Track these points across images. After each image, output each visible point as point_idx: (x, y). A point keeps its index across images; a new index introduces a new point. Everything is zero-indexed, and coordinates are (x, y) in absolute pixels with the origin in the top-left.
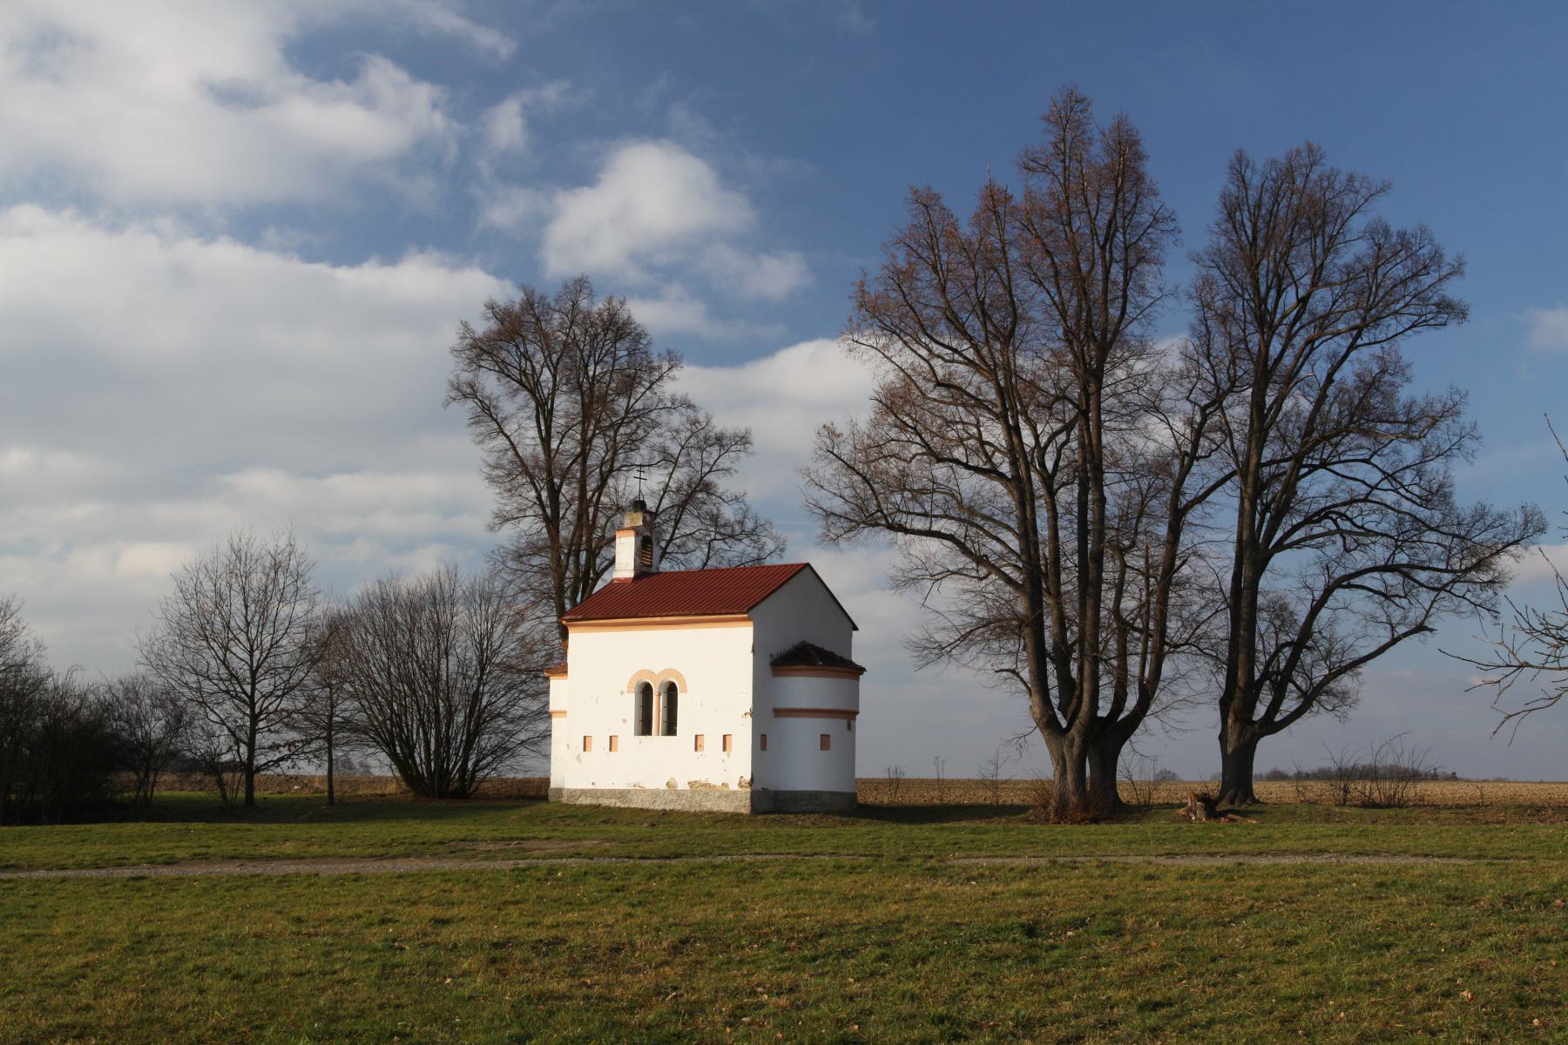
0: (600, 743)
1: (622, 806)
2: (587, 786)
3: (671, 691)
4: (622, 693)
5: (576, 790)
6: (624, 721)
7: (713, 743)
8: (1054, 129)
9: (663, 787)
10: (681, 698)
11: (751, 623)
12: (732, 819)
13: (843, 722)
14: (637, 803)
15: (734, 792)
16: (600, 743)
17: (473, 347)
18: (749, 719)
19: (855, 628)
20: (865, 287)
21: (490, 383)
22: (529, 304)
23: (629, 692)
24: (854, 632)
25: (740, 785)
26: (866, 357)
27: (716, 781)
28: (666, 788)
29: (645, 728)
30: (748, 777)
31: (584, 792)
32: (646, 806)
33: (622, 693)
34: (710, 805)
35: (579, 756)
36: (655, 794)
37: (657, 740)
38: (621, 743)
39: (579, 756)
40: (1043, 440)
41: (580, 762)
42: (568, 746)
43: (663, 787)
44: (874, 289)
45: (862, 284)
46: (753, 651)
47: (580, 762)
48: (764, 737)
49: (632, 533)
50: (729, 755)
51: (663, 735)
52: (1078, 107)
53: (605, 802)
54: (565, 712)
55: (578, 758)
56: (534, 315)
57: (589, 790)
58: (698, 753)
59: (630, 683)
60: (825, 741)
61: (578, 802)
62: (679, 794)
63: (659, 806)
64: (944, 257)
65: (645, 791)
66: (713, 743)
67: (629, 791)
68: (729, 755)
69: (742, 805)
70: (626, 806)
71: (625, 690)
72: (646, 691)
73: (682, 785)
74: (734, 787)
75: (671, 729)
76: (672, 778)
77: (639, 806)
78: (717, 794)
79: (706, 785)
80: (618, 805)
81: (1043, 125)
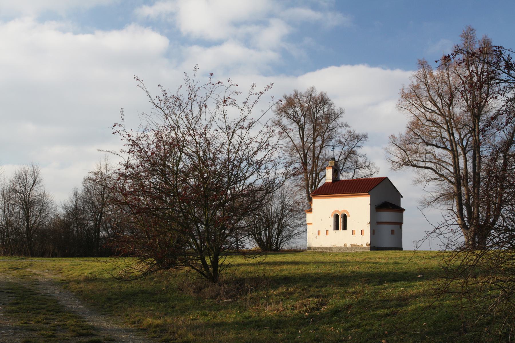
0: (323, 233)
3: (345, 217)
6: (330, 226)
8: (464, 39)
9: (343, 246)
10: (348, 219)
11: (369, 196)
13: (399, 226)
15: (365, 247)
16: (323, 233)
17: (279, 110)
18: (369, 225)
19: (402, 197)
20: (404, 91)
21: (285, 121)
22: (296, 95)
24: (402, 198)
25: (367, 245)
26: (404, 112)
29: (337, 228)
30: (369, 243)
37: (341, 232)
38: (329, 233)
40: (462, 137)
43: (343, 246)
44: (406, 91)
45: (403, 90)
46: (370, 204)
48: (374, 230)
49: (331, 168)
52: (471, 32)
54: (312, 224)
55: (316, 237)
56: (298, 99)
60: (393, 232)
62: (348, 248)
64: (429, 81)
65: (337, 247)
72: (337, 217)
73: (349, 245)
74: (365, 246)
75: (345, 228)
79: (356, 245)
81: (460, 38)
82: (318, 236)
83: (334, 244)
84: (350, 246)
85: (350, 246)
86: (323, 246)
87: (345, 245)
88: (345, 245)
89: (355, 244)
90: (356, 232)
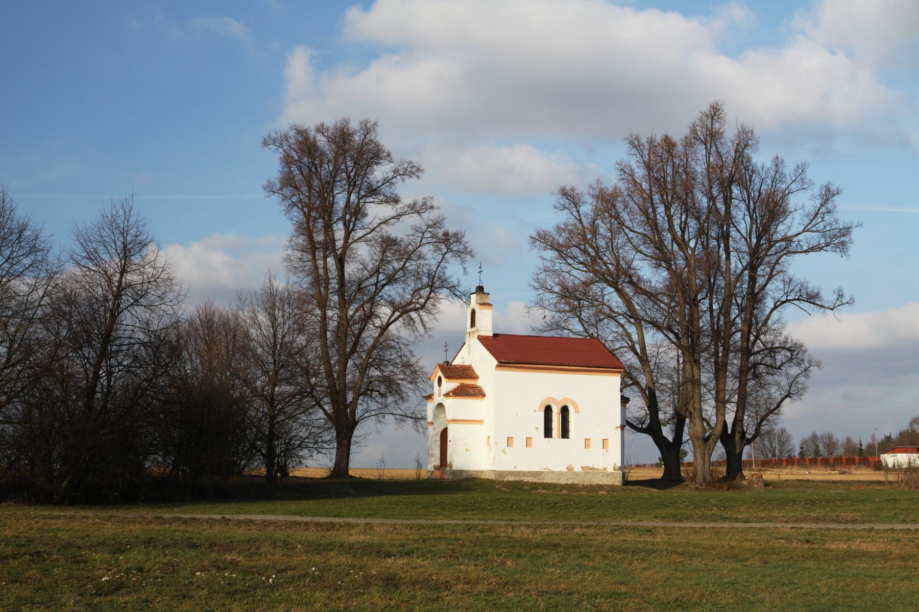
0: (519, 442)
1: (538, 481)
2: (511, 468)
3: (565, 411)
4: (535, 411)
5: (504, 472)
6: (537, 429)
7: (596, 444)
12: (612, 488)
14: (547, 480)
15: (613, 473)
16: (519, 442)
23: (539, 411)
25: (614, 469)
28: (566, 470)
29: (548, 433)
30: (619, 464)
31: (511, 473)
32: (554, 481)
33: (535, 411)
34: (596, 481)
35: (504, 450)
36: (560, 474)
38: (534, 442)
39: (504, 450)
41: (505, 453)
42: (496, 443)
47: (505, 453)
50: (607, 451)
51: (562, 438)
53: (526, 479)
55: (504, 451)
57: (515, 472)
58: (587, 450)
59: (540, 405)
61: (506, 479)
62: (577, 474)
65: (553, 472)
66: (596, 444)
67: (543, 472)
68: (607, 451)
69: (617, 481)
70: (541, 481)
71: (537, 409)
72: (548, 410)
73: (577, 469)
74: (611, 470)
75: (565, 433)
76: (570, 465)
77: (549, 481)
78: (601, 474)
79: (591, 469)
80: (534, 481)
82: (508, 449)
83: (546, 467)
84: (581, 470)
85: (581, 470)
87: (570, 469)
88: (570, 469)
89: (591, 465)
90: (592, 443)
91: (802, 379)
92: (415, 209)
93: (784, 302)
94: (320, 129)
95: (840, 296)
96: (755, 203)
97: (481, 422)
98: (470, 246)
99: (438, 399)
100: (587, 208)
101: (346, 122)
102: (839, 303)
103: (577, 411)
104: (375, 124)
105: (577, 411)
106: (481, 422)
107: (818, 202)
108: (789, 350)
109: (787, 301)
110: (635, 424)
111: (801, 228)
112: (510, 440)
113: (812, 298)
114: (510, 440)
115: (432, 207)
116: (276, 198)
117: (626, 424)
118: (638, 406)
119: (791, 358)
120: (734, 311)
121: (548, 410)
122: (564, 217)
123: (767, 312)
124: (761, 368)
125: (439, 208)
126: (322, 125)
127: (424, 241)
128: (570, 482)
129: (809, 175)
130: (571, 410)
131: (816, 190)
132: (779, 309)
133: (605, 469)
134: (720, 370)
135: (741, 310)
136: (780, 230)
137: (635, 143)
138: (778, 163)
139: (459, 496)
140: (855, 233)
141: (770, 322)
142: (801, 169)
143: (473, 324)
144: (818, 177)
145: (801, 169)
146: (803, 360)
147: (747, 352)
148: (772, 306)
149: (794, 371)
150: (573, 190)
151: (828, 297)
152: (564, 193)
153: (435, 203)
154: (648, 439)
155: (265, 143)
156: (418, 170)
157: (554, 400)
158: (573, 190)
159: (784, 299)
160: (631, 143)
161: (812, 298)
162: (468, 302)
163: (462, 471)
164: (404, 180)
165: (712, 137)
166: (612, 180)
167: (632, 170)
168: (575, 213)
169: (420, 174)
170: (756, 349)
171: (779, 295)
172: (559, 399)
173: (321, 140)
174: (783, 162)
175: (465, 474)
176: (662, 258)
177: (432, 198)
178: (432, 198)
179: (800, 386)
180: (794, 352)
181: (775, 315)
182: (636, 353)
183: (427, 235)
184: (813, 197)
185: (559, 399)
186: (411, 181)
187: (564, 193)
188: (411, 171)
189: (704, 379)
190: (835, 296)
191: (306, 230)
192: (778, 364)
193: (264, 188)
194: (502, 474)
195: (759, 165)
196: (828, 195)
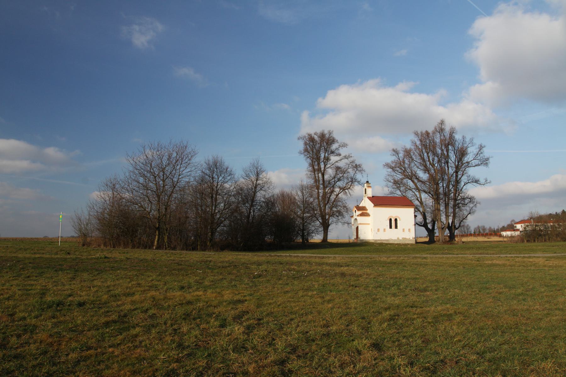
3: (396, 220)
7: (406, 230)
12: (412, 245)
14: (391, 242)
27: (408, 237)
29: (391, 227)
30: (414, 237)
31: (379, 240)
34: (407, 242)
36: (395, 240)
38: (386, 230)
43: (396, 239)
46: (550, 214)
53: (384, 242)
55: (377, 233)
62: (400, 240)
63: (396, 243)
66: (406, 230)
69: (414, 242)
72: (391, 220)
73: (400, 238)
74: (411, 239)
75: (396, 227)
77: (392, 243)
82: (378, 233)
86: (382, 239)
87: (398, 238)
88: (398, 238)
90: (405, 230)
91: (474, 208)
92: (346, 157)
93: (467, 183)
94: (315, 134)
95: (486, 180)
96: (456, 151)
97: (369, 224)
98: (364, 168)
99: (355, 217)
100: (401, 155)
101: (323, 131)
102: (486, 183)
103: (400, 220)
104: (332, 131)
105: (400, 220)
106: (369, 224)
107: (478, 150)
108: (469, 198)
109: (468, 183)
110: (419, 224)
111: (472, 159)
112: (378, 230)
113: (477, 181)
114: (378, 230)
115: (351, 157)
116: (302, 156)
117: (416, 224)
118: (420, 218)
119: (470, 201)
120: (451, 187)
121: (391, 220)
122: (394, 158)
123: (462, 187)
124: (460, 205)
125: (353, 157)
126: (316, 132)
127: (349, 167)
128: (398, 243)
129: (474, 141)
130: (398, 220)
131: (477, 146)
132: (466, 185)
133: (410, 238)
134: (447, 206)
135: (453, 186)
136: (466, 159)
137: (416, 134)
138: (464, 137)
139: (363, 248)
140: (491, 160)
141: (463, 190)
142: (472, 140)
143: (365, 193)
144: (477, 142)
145: (472, 140)
146: (474, 202)
147: (455, 200)
148: (463, 184)
149: (471, 205)
150: (396, 149)
151: (482, 181)
152: (394, 150)
153: (352, 155)
154: (423, 228)
155: (299, 139)
156: (347, 145)
157: (392, 217)
158: (396, 149)
159: (467, 182)
160: (415, 133)
161: (477, 181)
162: (364, 186)
163: (363, 240)
164: (342, 148)
165: (442, 130)
166: (409, 146)
167: (416, 142)
168: (397, 157)
169: (347, 146)
170: (458, 199)
171: (466, 181)
172: (394, 216)
173: (316, 137)
174: (465, 137)
175: (364, 241)
176: (426, 170)
177: (351, 154)
178: (351, 154)
179: (474, 210)
180: (471, 199)
181: (465, 187)
182: (419, 201)
183: (350, 165)
184: (476, 148)
185: (394, 216)
186: (344, 149)
187: (394, 150)
188: (344, 145)
189: (441, 209)
190: (485, 181)
191: (312, 165)
192: (466, 203)
193: (299, 153)
194: (376, 240)
195: (458, 139)
196: (481, 147)
